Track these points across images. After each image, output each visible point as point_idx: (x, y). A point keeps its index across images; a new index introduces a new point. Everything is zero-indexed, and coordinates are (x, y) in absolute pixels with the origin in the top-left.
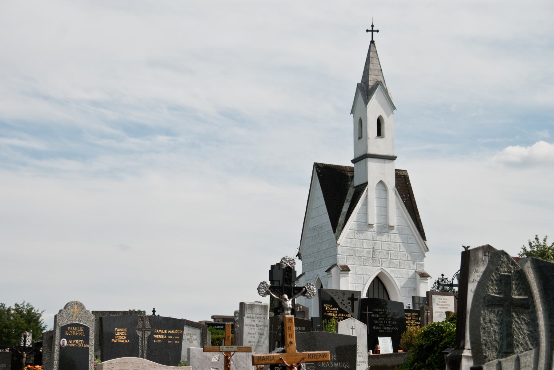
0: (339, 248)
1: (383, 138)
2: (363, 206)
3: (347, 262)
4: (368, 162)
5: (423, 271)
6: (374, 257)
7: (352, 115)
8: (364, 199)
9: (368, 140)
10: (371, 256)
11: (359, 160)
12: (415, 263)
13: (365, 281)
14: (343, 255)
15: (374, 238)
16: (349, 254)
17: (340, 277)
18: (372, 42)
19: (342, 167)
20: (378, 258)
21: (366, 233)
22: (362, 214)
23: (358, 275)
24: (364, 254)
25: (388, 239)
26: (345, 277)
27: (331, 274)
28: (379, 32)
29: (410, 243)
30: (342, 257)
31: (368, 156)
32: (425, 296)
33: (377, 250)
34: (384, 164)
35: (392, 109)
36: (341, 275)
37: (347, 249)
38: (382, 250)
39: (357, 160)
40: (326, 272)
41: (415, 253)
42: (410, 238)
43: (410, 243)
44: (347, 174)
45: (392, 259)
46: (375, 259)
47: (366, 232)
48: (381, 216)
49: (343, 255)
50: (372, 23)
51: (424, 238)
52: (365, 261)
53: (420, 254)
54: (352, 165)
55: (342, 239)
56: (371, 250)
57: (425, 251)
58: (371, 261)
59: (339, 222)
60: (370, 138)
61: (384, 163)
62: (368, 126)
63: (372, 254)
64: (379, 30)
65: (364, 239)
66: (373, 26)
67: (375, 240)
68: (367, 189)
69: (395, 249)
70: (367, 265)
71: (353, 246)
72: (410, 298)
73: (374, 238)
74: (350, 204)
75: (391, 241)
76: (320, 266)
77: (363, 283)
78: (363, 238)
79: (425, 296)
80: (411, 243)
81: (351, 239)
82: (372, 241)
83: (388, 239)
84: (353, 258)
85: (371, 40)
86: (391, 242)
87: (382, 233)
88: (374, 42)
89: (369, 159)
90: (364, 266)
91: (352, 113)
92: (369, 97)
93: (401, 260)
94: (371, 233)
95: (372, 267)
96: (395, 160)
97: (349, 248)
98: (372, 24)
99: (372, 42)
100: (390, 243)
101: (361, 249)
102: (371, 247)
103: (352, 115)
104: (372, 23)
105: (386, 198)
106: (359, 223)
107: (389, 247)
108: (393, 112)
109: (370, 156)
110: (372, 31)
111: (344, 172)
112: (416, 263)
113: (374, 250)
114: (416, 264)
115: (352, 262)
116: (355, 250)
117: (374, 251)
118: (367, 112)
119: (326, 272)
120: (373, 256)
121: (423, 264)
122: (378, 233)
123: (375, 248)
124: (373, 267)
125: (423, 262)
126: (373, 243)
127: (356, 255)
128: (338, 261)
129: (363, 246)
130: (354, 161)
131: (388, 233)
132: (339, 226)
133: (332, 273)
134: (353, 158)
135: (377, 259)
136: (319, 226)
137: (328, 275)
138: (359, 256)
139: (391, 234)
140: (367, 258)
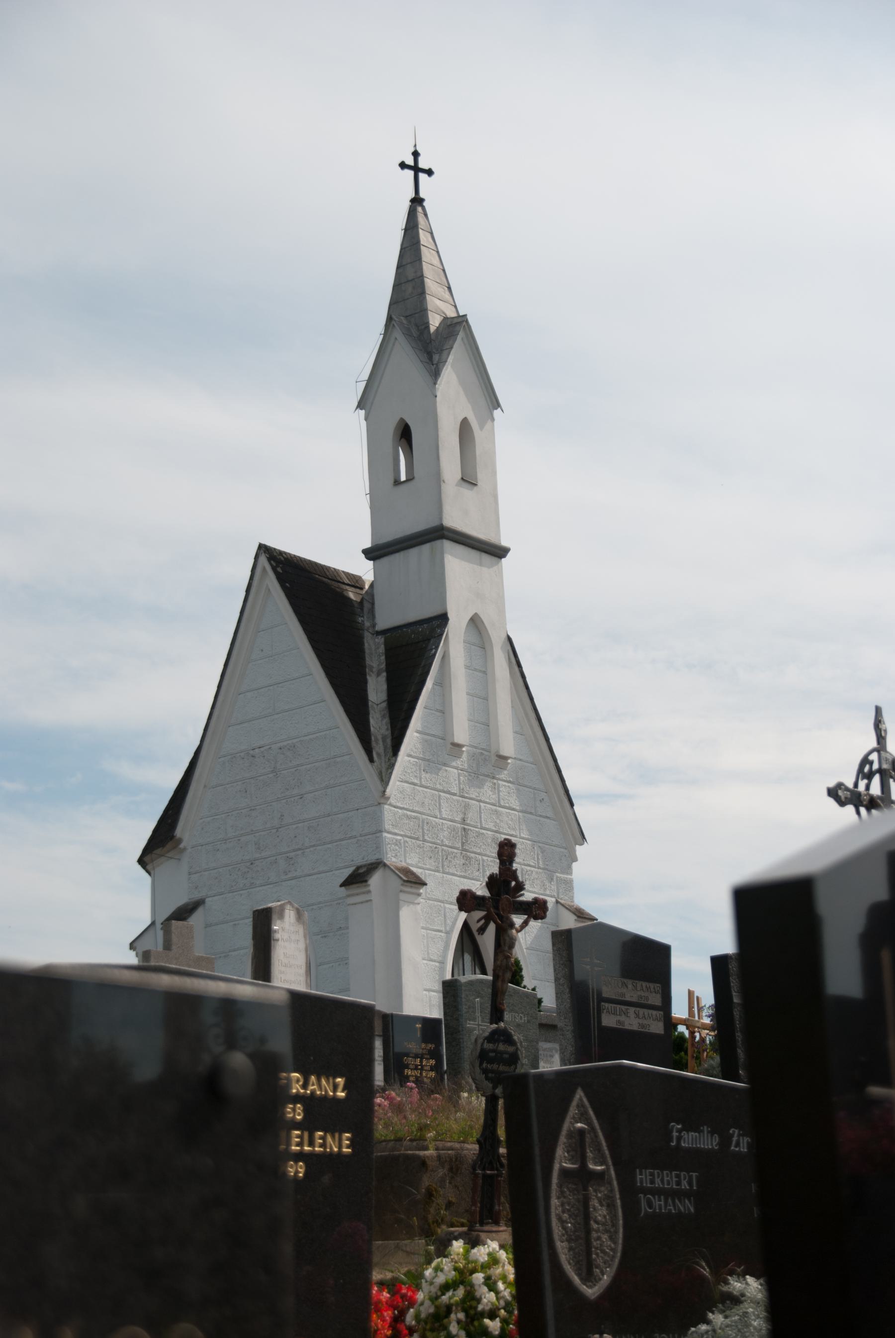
0: (388, 812)
1: (475, 488)
2: (435, 687)
3: (405, 857)
4: (445, 555)
5: (573, 902)
6: (466, 850)
7: (362, 413)
8: (438, 666)
9: (443, 486)
10: (459, 845)
11: (393, 548)
12: (553, 876)
13: (449, 922)
14: (396, 834)
15: (463, 789)
16: (408, 834)
17: (401, 903)
18: (417, 201)
19: (328, 569)
20: (475, 853)
21: (446, 771)
22: (434, 712)
23: (431, 902)
24: (444, 836)
25: (494, 796)
26: (411, 906)
27: (369, 892)
28: (433, 177)
29: (540, 816)
30: (394, 841)
31: (446, 533)
32: (435, 1011)
33: (472, 828)
34: (479, 567)
35: (491, 408)
36: (402, 896)
37: (404, 815)
38: (482, 828)
39: (390, 549)
40: (341, 886)
41: (553, 848)
42: (541, 801)
43: (540, 816)
44: (345, 593)
45: (448, 873)
46: (468, 854)
47: (447, 768)
48: (477, 724)
49: (396, 834)
50: (415, 146)
51: (572, 805)
52: (447, 858)
53: (562, 850)
54: (365, 570)
55: (395, 786)
56: (459, 825)
57: (576, 844)
58: (460, 861)
59: (372, 729)
60: (446, 481)
61: (481, 564)
62: (440, 445)
63: (462, 839)
64: (433, 170)
65: (441, 788)
66: (416, 154)
67: (466, 795)
68: (448, 631)
69: (509, 827)
70: (451, 871)
71: (417, 809)
72: (547, 984)
73: (463, 789)
74: (389, 681)
75: (502, 803)
76: (286, 873)
77: (443, 929)
78: (438, 786)
79: (435, 1011)
80: (544, 814)
81: (413, 786)
82: (461, 799)
83: (494, 798)
84: (419, 846)
85: (412, 195)
86: (501, 806)
87: (481, 777)
88: (422, 200)
89: (447, 544)
90: (445, 875)
91: (361, 405)
92: (436, 357)
93: (525, 865)
94: (456, 771)
95: (462, 879)
96: (503, 559)
97: (409, 813)
98: (413, 150)
99: (417, 201)
100: (498, 808)
101: (434, 819)
102: (458, 818)
103: (362, 413)
104: (415, 146)
105: (484, 669)
106: (429, 738)
107: (498, 821)
108: (492, 415)
109: (451, 535)
110: (416, 169)
111: (336, 584)
112: (557, 877)
113: (466, 827)
114: (557, 880)
115: (417, 859)
116: (423, 822)
117: (464, 829)
118: (438, 399)
119: (341, 886)
120: (463, 844)
121: (571, 881)
122: (473, 775)
123: (468, 822)
124: (465, 880)
125: (569, 877)
126: (463, 804)
127: (426, 837)
128: (387, 854)
129: (440, 812)
130: (371, 554)
131: (494, 778)
132: (377, 743)
133: (371, 888)
134: (368, 544)
135: (473, 855)
136: (279, 745)
137: (348, 896)
138: (432, 843)
139: (500, 782)
140: (450, 850)
